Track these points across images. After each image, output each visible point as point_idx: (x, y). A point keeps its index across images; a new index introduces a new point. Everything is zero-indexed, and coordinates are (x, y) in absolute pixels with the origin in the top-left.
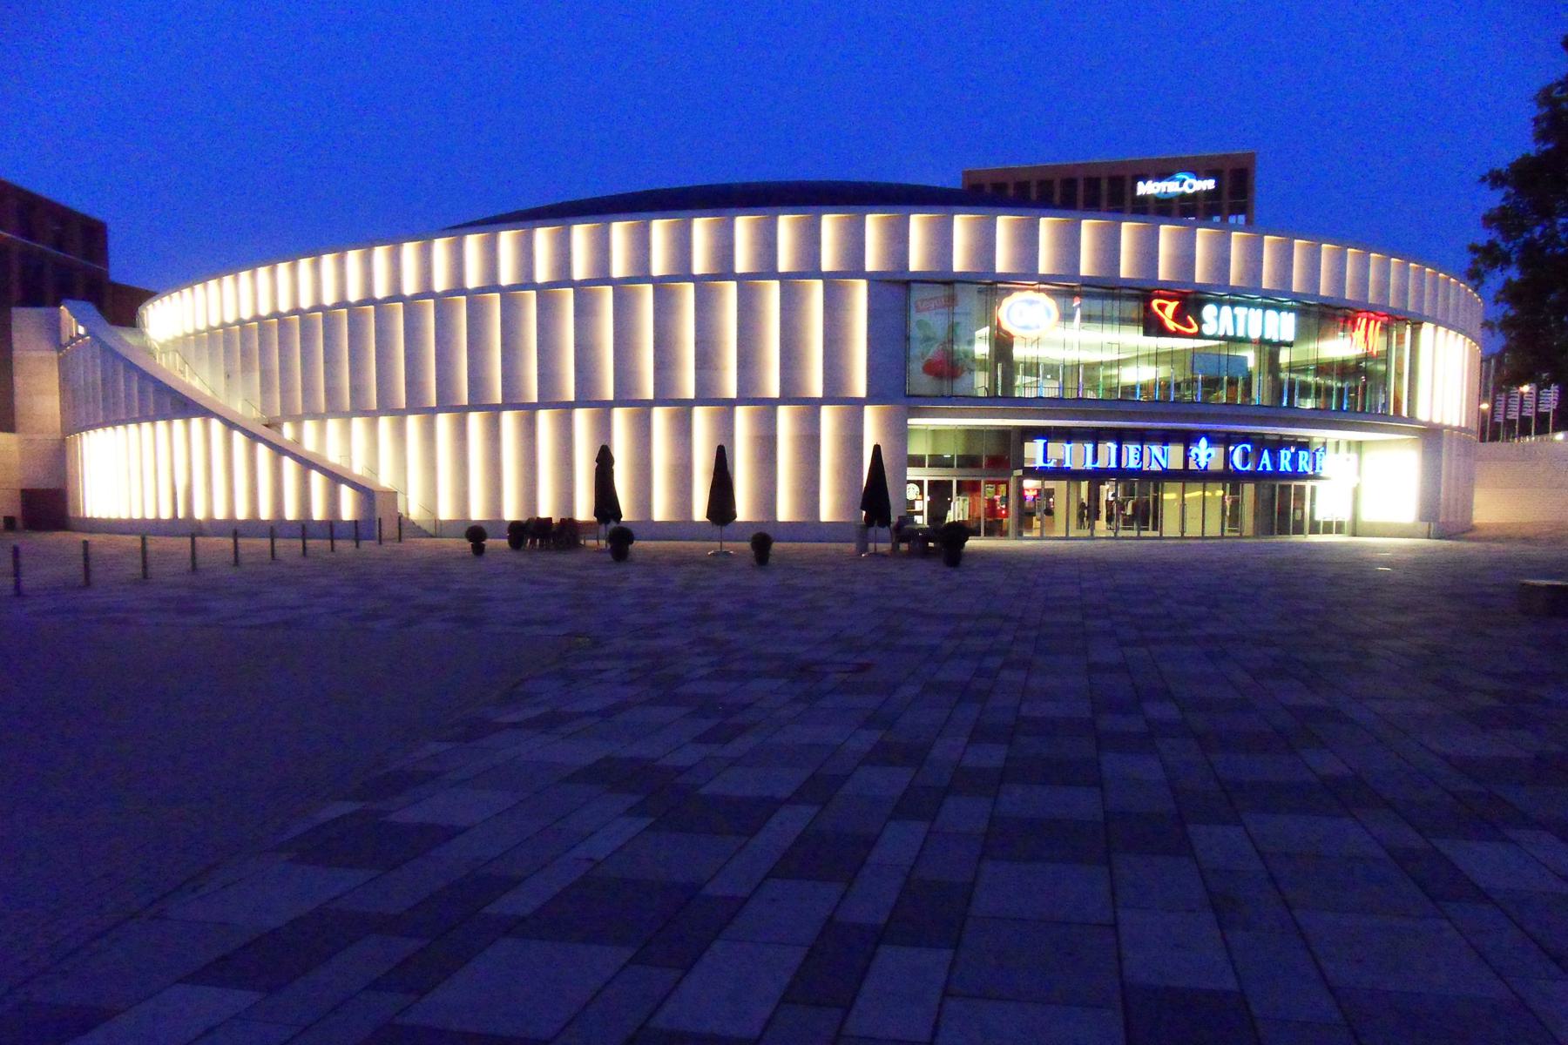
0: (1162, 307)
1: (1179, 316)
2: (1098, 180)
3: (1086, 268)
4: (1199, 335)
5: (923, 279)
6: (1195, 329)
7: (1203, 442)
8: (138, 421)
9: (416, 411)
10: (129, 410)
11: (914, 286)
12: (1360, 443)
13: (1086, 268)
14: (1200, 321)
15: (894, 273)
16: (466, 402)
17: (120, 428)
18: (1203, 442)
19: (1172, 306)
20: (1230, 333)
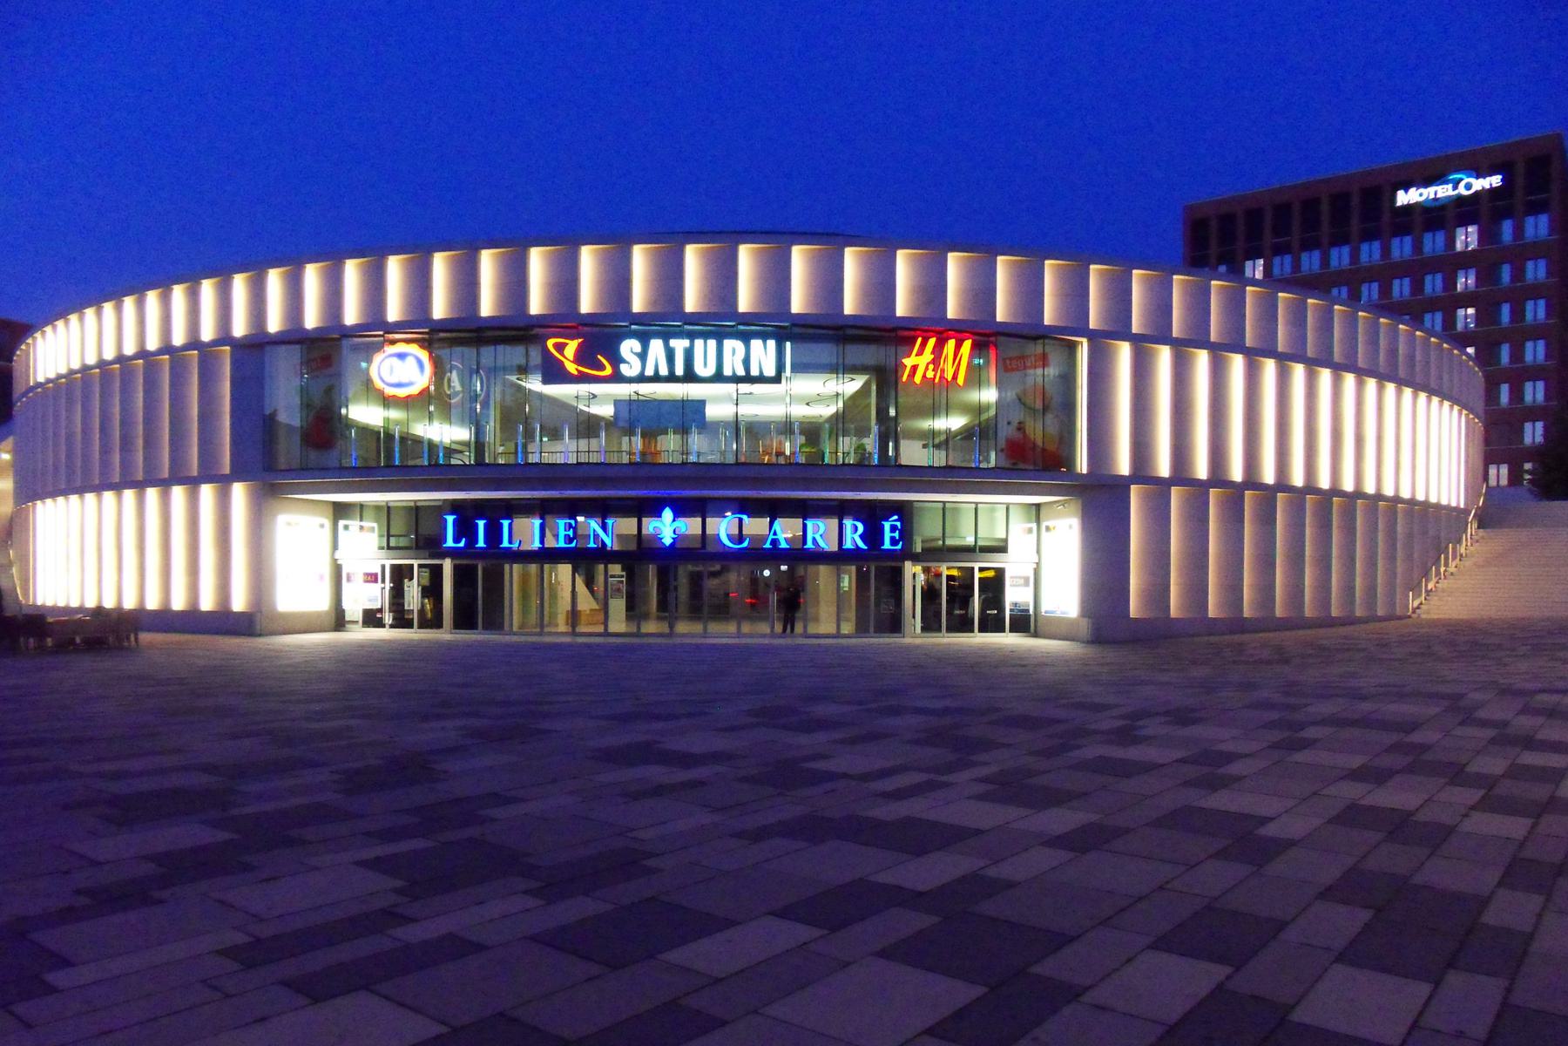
0: (560, 348)
1: (579, 358)
2: (1317, 201)
3: (487, 307)
4: (617, 378)
5: (281, 340)
6: (608, 371)
7: (668, 514)
8: (99, 489)
9: (180, 482)
10: (69, 480)
11: (268, 348)
12: (1038, 506)
13: (798, 303)
14: (616, 360)
15: (923, 320)
16: (195, 473)
17: (61, 499)
18: (668, 514)
19: (572, 346)
20: (741, 372)
